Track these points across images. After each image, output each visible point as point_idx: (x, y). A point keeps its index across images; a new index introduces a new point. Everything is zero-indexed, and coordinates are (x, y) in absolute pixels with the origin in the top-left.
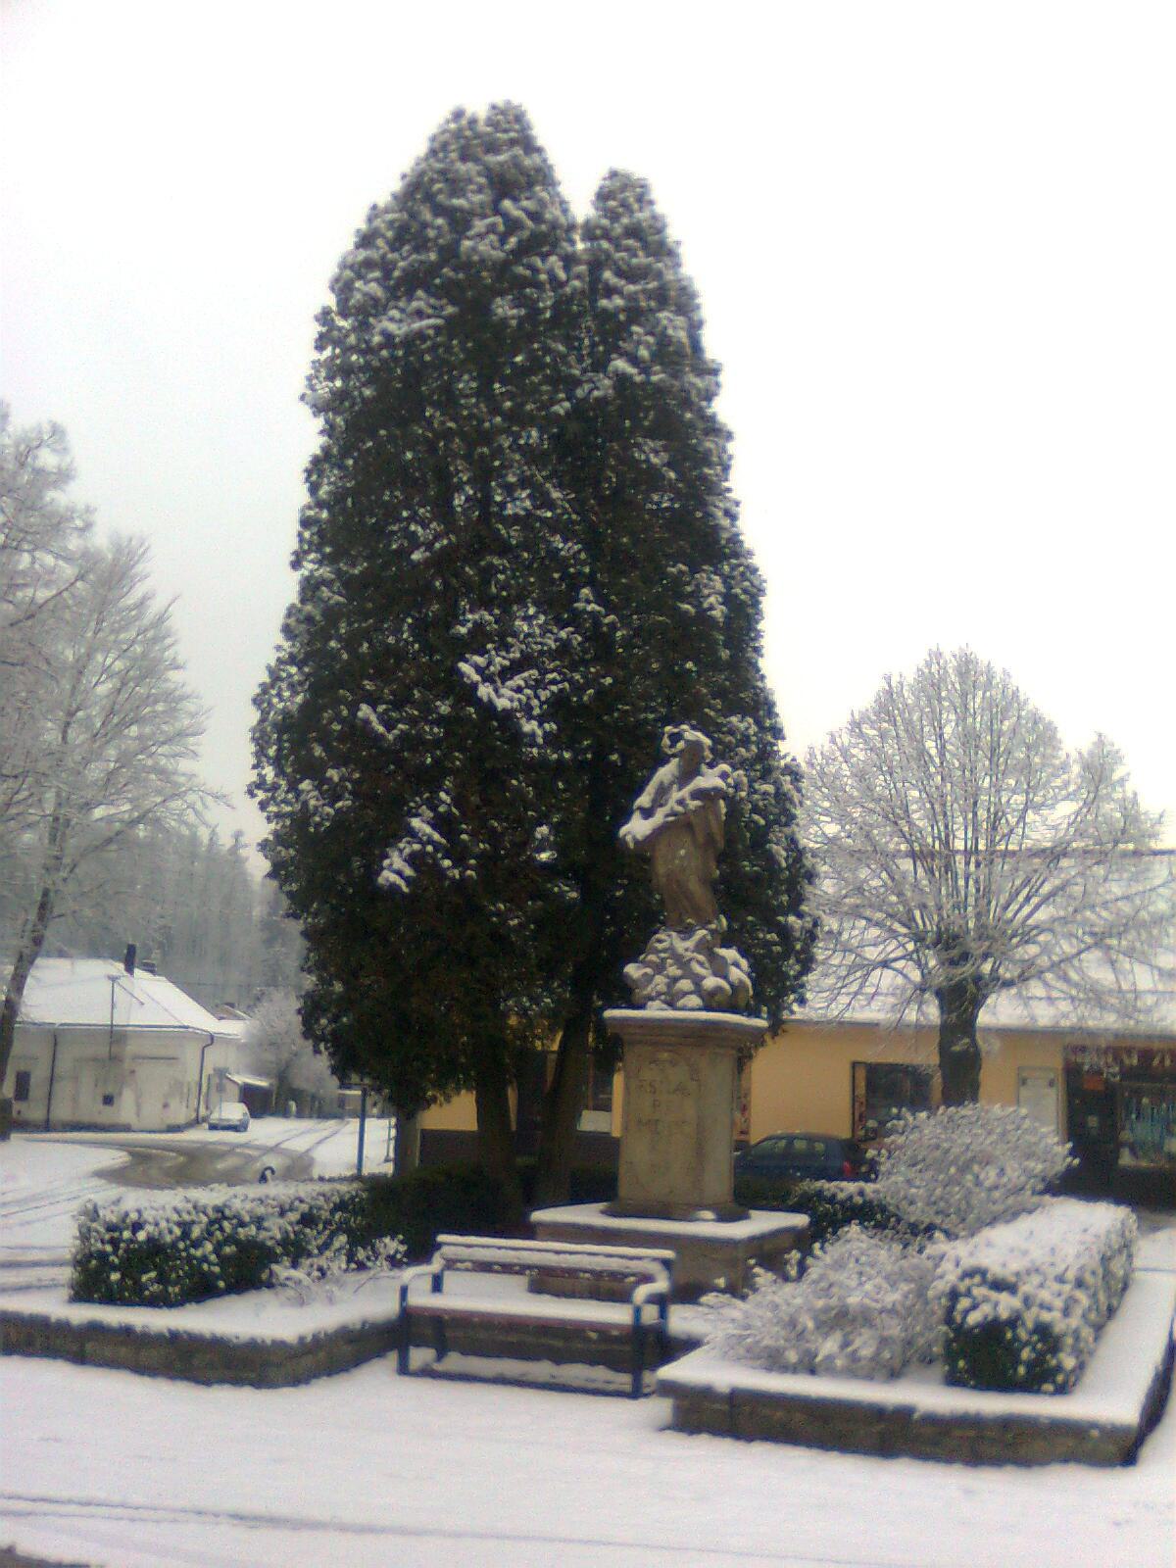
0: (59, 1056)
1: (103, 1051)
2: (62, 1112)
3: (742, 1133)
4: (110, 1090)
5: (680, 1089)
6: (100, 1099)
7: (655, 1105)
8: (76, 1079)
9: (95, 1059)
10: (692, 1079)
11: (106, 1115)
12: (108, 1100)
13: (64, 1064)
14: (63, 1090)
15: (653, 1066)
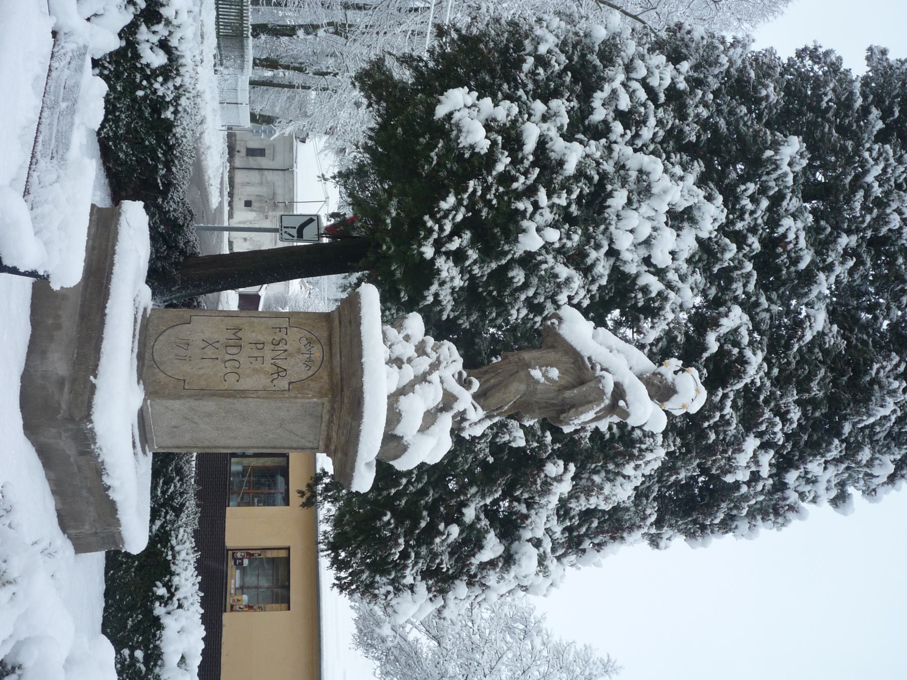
0: (275, 172)
1: (280, 198)
2: (240, 176)
3: (232, 606)
4: (255, 205)
5: (280, 371)
6: (249, 199)
7: (259, 345)
8: (261, 184)
9: (274, 194)
10: (290, 383)
11: (239, 204)
12: (248, 204)
13: (270, 176)
14: (254, 176)
15: (304, 341)
